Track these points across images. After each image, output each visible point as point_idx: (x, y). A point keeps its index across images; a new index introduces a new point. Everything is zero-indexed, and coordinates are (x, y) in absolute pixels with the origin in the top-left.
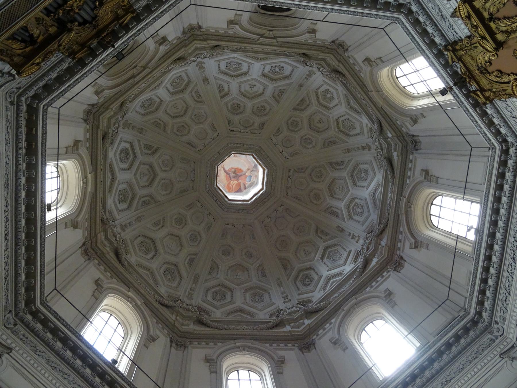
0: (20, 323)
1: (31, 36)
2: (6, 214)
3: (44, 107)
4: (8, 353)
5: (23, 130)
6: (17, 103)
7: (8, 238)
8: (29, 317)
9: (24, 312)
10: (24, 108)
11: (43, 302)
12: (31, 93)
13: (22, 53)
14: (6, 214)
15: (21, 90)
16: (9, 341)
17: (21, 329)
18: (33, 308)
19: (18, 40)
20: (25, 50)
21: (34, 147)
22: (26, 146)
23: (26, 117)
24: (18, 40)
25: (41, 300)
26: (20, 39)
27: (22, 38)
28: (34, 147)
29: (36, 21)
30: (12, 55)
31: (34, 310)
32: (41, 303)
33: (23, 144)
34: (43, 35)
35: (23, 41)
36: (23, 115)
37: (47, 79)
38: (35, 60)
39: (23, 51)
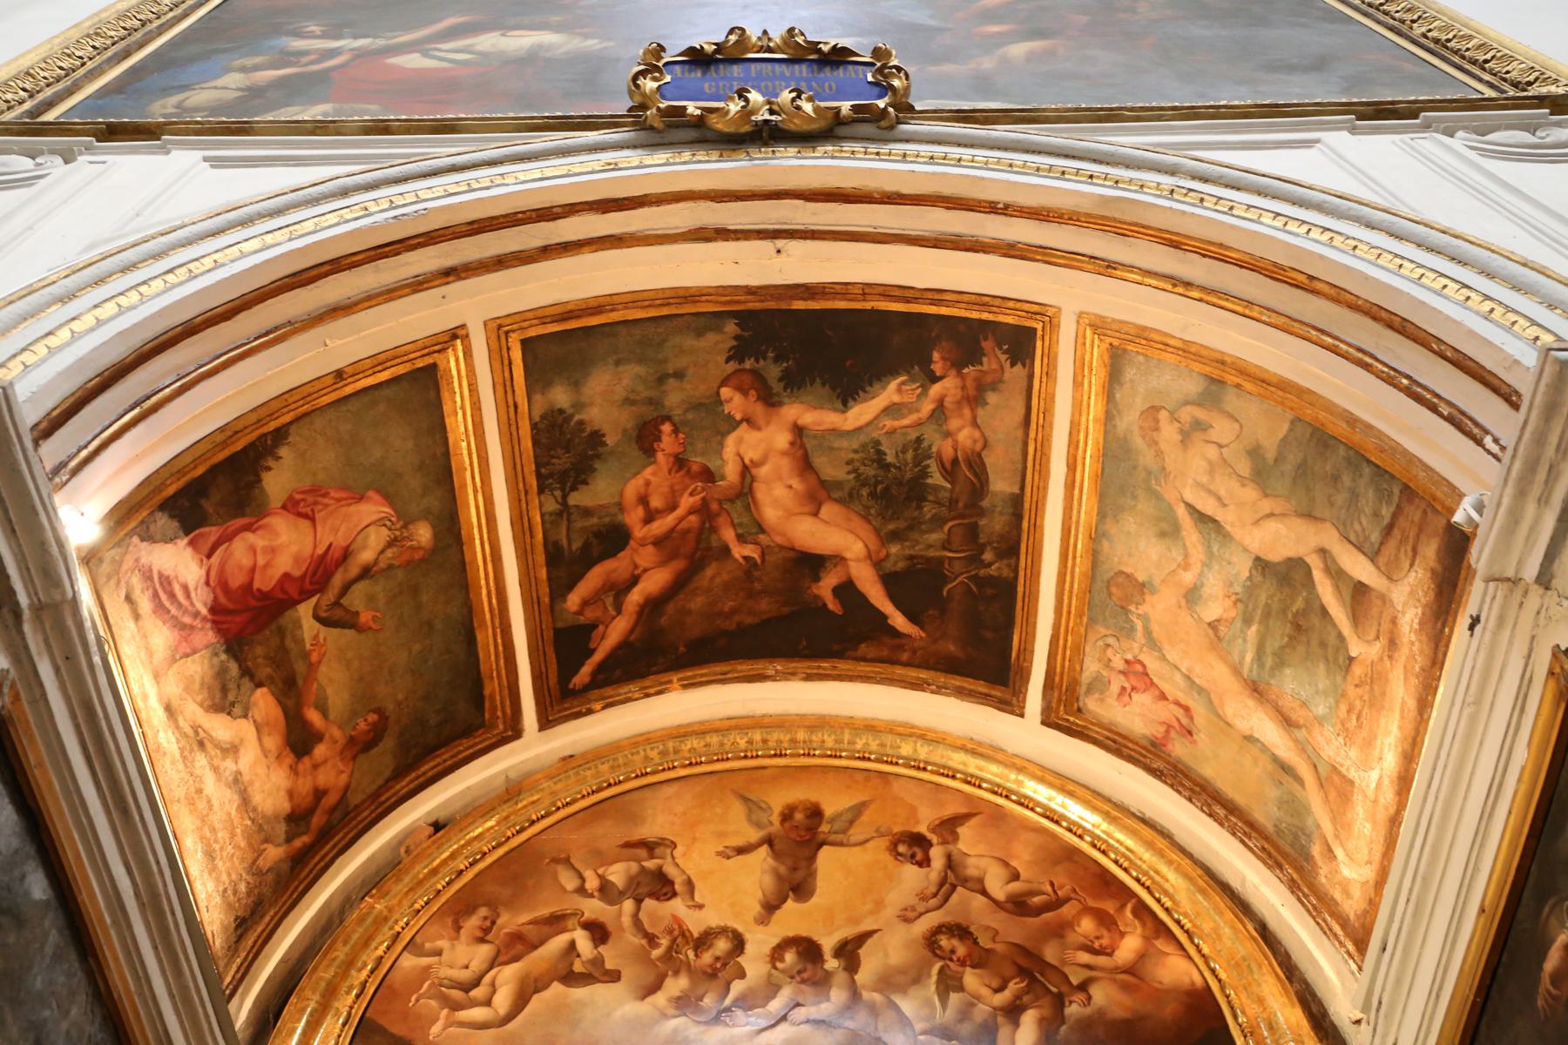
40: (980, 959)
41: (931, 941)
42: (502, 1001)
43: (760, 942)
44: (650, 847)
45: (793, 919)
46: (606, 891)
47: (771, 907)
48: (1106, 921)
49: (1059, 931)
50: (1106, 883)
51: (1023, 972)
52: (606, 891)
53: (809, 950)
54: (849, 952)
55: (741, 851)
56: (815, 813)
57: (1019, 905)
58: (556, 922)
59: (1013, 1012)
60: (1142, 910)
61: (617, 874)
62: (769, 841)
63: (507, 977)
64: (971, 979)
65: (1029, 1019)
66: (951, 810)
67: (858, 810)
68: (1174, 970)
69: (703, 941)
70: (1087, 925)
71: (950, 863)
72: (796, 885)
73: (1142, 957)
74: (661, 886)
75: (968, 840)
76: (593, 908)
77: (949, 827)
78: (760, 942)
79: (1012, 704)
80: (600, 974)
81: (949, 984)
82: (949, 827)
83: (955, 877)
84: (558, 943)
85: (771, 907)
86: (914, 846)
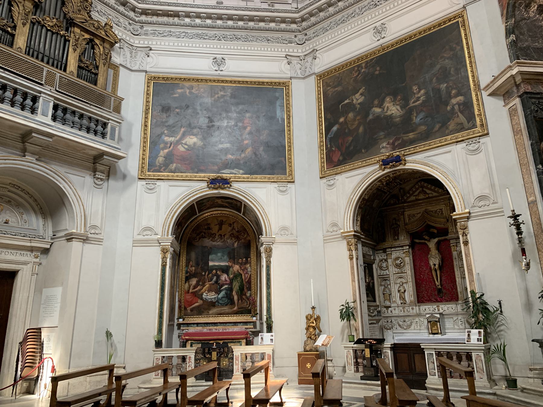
0: (306, 31)
1: (88, 44)
2: (221, 37)
3: (139, 3)
4: (317, 51)
5: (161, 19)
6: (141, 23)
7: (239, 37)
8: (304, 24)
9: (300, 26)
10: (143, 18)
11: (297, 11)
12: (132, 14)
13: (101, 45)
14: (221, 37)
15: (131, 22)
16: (311, 46)
17: (310, 32)
18: (298, 20)
19: (94, 52)
20: (98, 44)
21: (172, 13)
22: (172, 18)
23: (150, 17)
24: (94, 52)
25: (295, 13)
26: (92, 50)
27: (92, 49)
28: (172, 13)
29: (76, 50)
30: (105, 54)
31: (300, 19)
32: (297, 13)
33: (171, 20)
34: (84, 36)
35: (93, 48)
36: (149, 19)
37: (116, 6)
38: (103, 35)
39: (100, 46)
40: (234, 237)
41: (230, 235)
42: (198, 239)
43: (217, 234)
44: (209, 224)
45: (220, 232)
46: (205, 229)
47: (218, 231)
48: (244, 233)
49: (240, 234)
50: (245, 230)
51: (237, 238)
52: (205, 229)
53: (221, 235)
54: (224, 236)
55: (216, 225)
56: (222, 221)
57: (238, 232)
58: (201, 232)
59: (236, 242)
60: (247, 233)
61: (206, 227)
62: (218, 224)
63: (198, 237)
64: (233, 239)
65: (237, 242)
66: (234, 221)
67: (226, 221)
68: (248, 238)
69: (213, 234)
70: (243, 234)
71: (233, 227)
72: (220, 229)
73: (247, 237)
74: (209, 229)
75: (235, 225)
76: (204, 231)
77: (233, 223)
78: (217, 234)
79: (240, 213)
80: (205, 237)
81: (231, 239)
82: (233, 223)
83: (233, 229)
84: (202, 234)
85: (218, 231)
86: (230, 225)
